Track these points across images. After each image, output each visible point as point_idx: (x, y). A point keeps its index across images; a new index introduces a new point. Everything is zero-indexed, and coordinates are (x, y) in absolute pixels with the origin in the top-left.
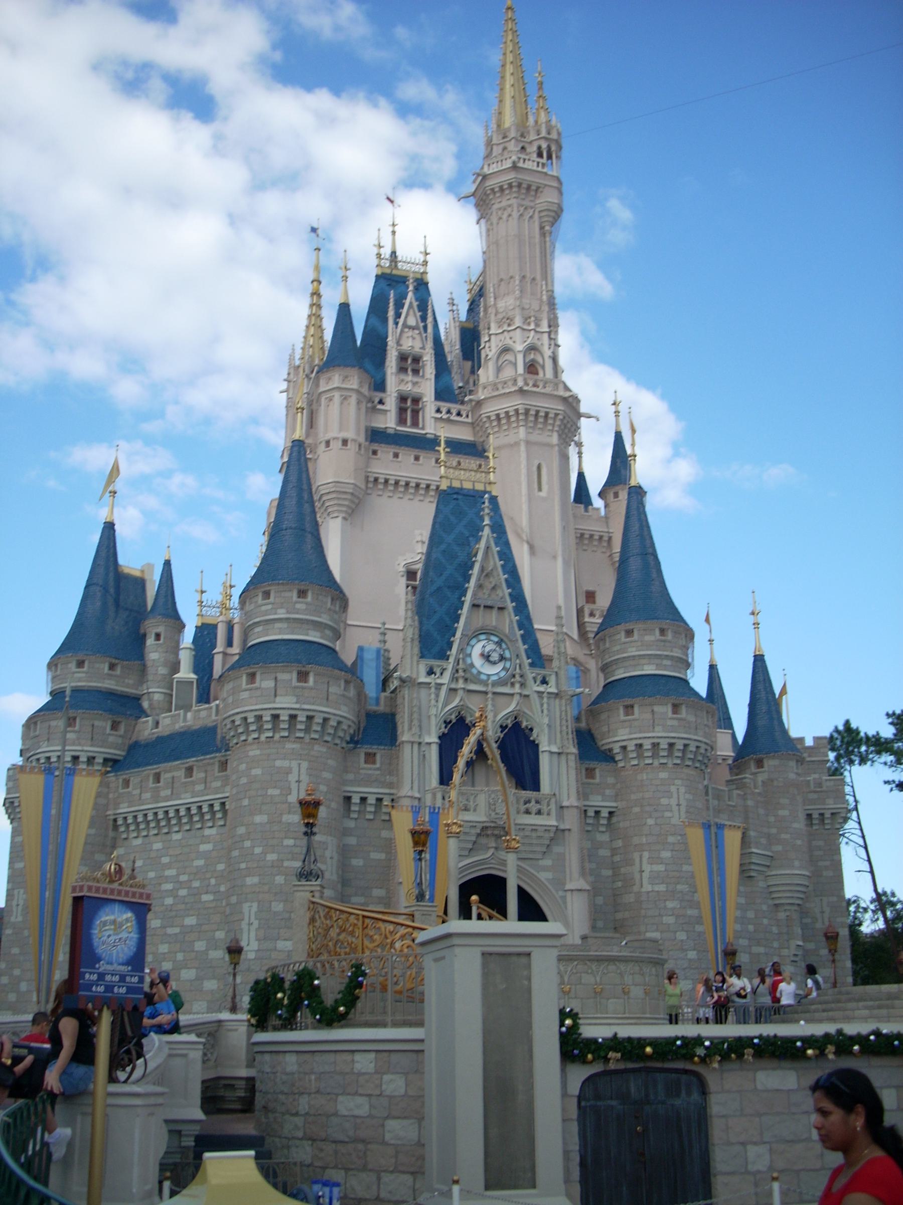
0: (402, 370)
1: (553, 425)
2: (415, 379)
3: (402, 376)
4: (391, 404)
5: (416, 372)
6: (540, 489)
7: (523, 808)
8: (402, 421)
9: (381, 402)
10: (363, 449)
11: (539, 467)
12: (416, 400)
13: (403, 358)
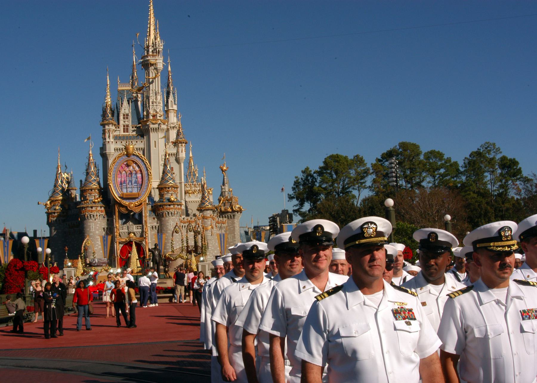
0: (124, 118)
1: (158, 130)
2: (127, 120)
3: (124, 120)
4: (122, 128)
5: (127, 118)
6: (155, 147)
7: (137, 228)
8: (124, 132)
9: (119, 128)
10: (113, 143)
11: (155, 141)
12: (128, 126)
13: (124, 115)
